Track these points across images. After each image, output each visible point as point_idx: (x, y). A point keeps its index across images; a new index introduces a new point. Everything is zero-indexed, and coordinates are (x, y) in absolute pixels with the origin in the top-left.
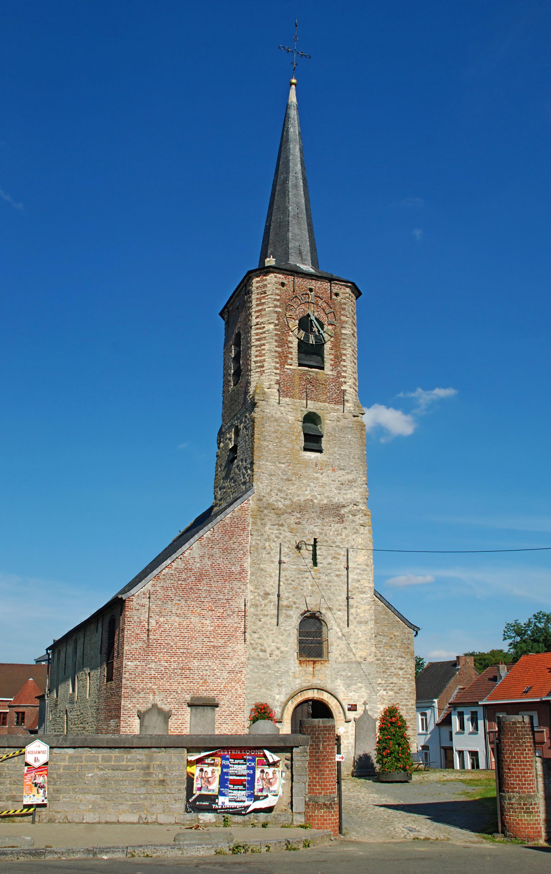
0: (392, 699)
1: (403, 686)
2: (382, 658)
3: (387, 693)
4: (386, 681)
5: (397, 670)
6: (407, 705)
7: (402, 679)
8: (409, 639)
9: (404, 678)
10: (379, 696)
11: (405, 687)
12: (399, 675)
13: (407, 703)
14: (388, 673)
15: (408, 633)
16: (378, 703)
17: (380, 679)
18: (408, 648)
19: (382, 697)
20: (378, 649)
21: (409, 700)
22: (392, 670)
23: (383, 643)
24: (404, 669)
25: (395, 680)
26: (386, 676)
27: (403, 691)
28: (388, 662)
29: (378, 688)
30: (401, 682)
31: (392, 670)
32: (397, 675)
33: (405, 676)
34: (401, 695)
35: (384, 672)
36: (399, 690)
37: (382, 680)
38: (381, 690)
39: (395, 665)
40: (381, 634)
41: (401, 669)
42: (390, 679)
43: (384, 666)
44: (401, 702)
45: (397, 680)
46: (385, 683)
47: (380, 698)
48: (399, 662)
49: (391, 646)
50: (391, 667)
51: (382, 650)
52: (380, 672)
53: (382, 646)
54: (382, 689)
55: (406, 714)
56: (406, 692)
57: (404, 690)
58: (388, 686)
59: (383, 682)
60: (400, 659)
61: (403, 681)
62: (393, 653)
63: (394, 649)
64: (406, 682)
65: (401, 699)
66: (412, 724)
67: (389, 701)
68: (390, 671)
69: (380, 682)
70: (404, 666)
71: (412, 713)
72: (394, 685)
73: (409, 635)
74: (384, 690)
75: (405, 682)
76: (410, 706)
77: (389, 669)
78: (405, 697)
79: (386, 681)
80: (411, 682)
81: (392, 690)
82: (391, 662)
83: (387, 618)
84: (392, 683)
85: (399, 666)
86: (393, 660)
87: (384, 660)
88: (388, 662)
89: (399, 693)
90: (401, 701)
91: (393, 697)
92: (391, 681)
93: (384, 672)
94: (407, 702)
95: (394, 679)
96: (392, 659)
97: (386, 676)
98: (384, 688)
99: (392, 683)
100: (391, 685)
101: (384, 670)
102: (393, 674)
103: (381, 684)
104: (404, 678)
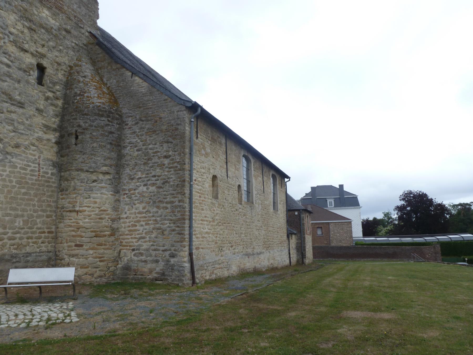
0: (154, 196)
1: (168, 178)
2: (144, 147)
3: (147, 189)
4: (147, 174)
5: (162, 159)
6: (172, 202)
7: (167, 169)
8: (178, 118)
9: (169, 168)
10: (138, 193)
11: (171, 179)
12: (164, 165)
13: (172, 199)
14: (151, 165)
15: (178, 111)
16: (136, 202)
17: (140, 173)
18: (177, 129)
19: (142, 195)
20: (140, 137)
21: (175, 195)
22: (155, 160)
23: (145, 130)
24: (170, 156)
25: (158, 171)
26: (147, 168)
27: (168, 184)
28: (151, 151)
29: (138, 184)
30: (166, 173)
31: (155, 160)
32: (162, 166)
33: (171, 165)
34: (165, 189)
35: (145, 164)
36: (163, 183)
37: (142, 174)
38: (141, 185)
39: (159, 154)
40: (144, 119)
41: (166, 157)
42: (152, 171)
43: (145, 156)
44: (164, 199)
45: (161, 171)
46: (146, 177)
47: (138, 196)
48: (165, 149)
49: (155, 131)
50: (154, 156)
51: (143, 137)
52: (141, 165)
53: (144, 132)
54: (142, 184)
55: (171, 214)
56: (171, 186)
57: (169, 183)
58: (148, 181)
59: (144, 176)
60: (165, 145)
61: (168, 172)
62: (157, 139)
63: (158, 134)
64: (173, 172)
65: (165, 195)
66: (178, 227)
67: (150, 199)
68: (153, 161)
69: (140, 176)
70: (170, 153)
71: (179, 212)
72: (157, 178)
73: (179, 113)
74: (145, 185)
75: (171, 173)
76: (177, 203)
77: (151, 160)
78: (171, 192)
79: (147, 174)
80: (179, 172)
81: (153, 185)
82: (154, 151)
83: (152, 98)
84: (154, 176)
85: (165, 154)
86: (157, 148)
87: (146, 149)
88: (151, 151)
89: (163, 188)
90: (164, 197)
91: (155, 193)
92: (153, 174)
93: (145, 164)
94: (173, 198)
95: (158, 170)
96: (156, 146)
97: (147, 168)
98: (144, 183)
99: (154, 176)
100: (154, 179)
101: (146, 161)
102: (156, 164)
103: (140, 178)
104: (169, 168)
